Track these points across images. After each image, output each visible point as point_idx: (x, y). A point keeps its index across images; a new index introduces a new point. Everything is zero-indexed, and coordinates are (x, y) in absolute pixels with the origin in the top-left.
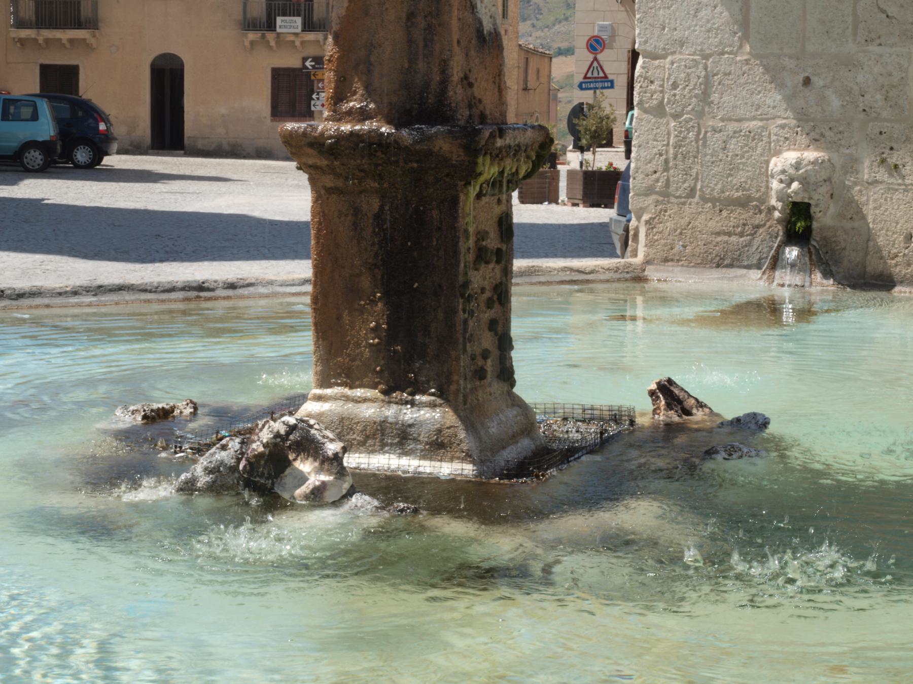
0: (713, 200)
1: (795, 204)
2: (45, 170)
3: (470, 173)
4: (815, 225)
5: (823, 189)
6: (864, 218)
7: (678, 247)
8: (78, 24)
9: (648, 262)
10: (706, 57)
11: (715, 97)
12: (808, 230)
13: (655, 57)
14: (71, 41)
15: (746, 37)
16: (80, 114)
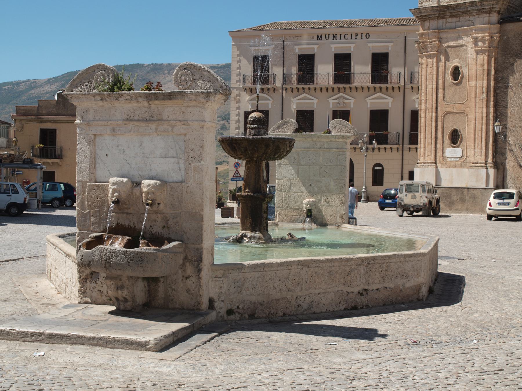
0: (292, 209)
1: (308, 209)
2: (59, 208)
3: (265, 200)
4: (312, 214)
5: (314, 206)
6: (322, 212)
7: (285, 218)
8: (55, 157)
9: (279, 222)
10: (290, 180)
11: (292, 188)
12: (311, 215)
13: (280, 180)
14: (52, 163)
15: (298, 176)
16: (68, 189)
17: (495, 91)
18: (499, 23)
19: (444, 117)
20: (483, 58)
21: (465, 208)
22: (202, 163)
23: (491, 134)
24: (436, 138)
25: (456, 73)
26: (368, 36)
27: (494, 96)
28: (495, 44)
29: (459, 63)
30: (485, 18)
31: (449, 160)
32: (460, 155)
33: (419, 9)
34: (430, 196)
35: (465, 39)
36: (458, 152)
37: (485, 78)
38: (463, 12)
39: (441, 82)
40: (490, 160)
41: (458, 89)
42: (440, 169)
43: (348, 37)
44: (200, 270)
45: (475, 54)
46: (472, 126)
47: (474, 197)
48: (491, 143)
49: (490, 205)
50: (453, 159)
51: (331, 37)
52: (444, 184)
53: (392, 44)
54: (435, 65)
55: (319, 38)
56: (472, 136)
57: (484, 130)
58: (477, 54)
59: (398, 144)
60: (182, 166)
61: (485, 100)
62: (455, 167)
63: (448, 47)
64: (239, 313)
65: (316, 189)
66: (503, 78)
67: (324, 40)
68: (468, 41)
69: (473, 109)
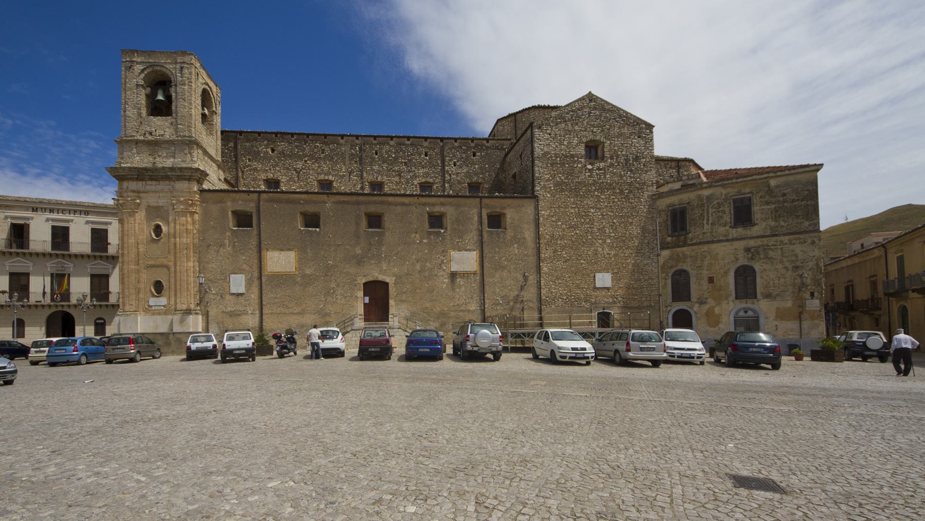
36: (163, 301)
62: (160, 314)
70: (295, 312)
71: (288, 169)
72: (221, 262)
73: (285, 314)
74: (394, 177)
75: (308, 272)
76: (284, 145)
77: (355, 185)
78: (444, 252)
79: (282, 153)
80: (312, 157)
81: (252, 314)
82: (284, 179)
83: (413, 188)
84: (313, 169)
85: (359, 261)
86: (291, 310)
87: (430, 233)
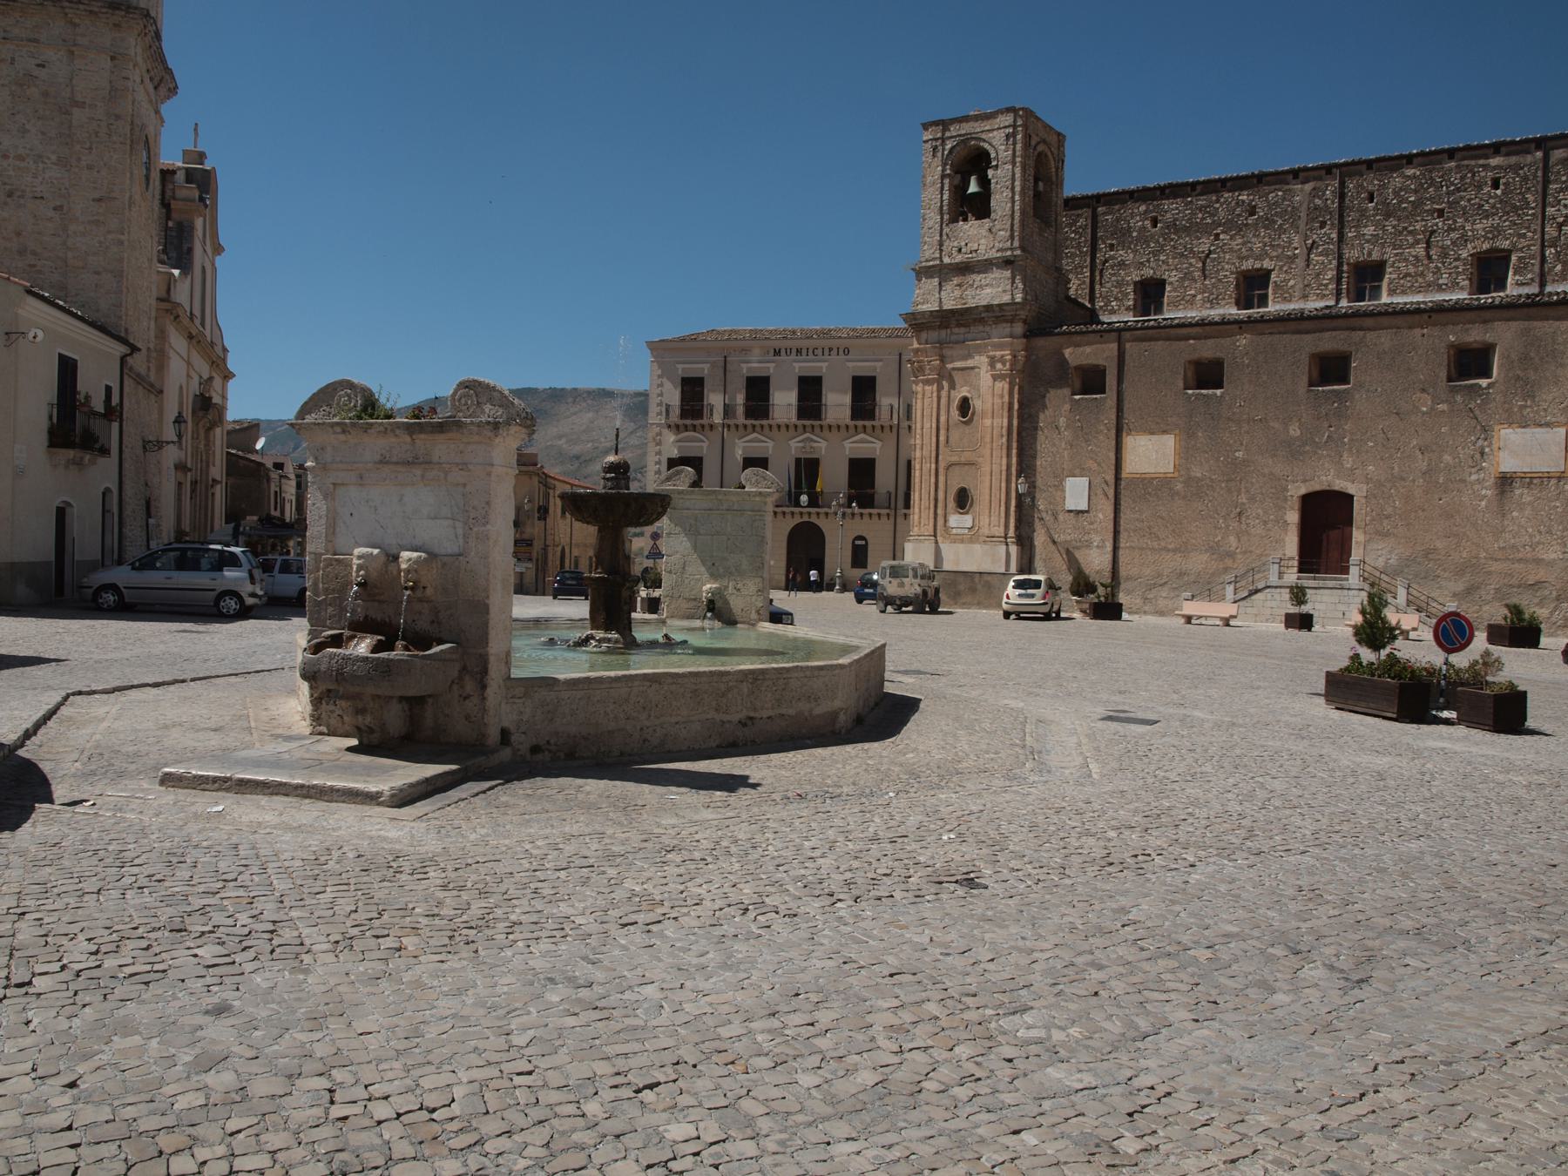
12: (714, 608)
17: (1019, 434)
18: (1025, 336)
19: (947, 469)
20: (1003, 386)
21: (976, 602)
22: (489, 527)
23: (1013, 495)
24: (936, 500)
25: (965, 405)
26: (847, 351)
27: (1018, 441)
28: (1019, 366)
29: (969, 392)
30: (1005, 328)
31: (954, 531)
32: (969, 524)
33: (913, 314)
34: (924, 583)
35: (977, 358)
36: (967, 520)
37: (1006, 414)
38: (975, 320)
39: (943, 419)
40: (1011, 533)
41: (967, 429)
42: (941, 546)
43: (819, 352)
44: (484, 687)
45: (991, 380)
46: (988, 484)
47: (988, 585)
48: (1013, 508)
49: (1008, 597)
50: (959, 531)
51: (794, 351)
52: (947, 566)
53: (881, 363)
54: (935, 394)
55: (777, 353)
56: (987, 497)
57: (1004, 490)
58: (995, 380)
59: (889, 507)
60: (460, 531)
61: (1005, 447)
62: (962, 541)
63: (954, 369)
64: (550, 751)
65: (721, 570)
66: (1030, 416)
67: (783, 357)
68: (981, 361)
69: (988, 459)
70: (1170, 547)
71: (1182, 255)
72: (1054, 455)
73: (1153, 549)
74: (1412, 246)
75: (1197, 472)
76: (1177, 208)
77: (1318, 274)
78: (1486, 431)
79: (1173, 227)
80: (1229, 226)
81: (1098, 547)
82: (1172, 277)
83: (1457, 267)
84: (1231, 250)
85: (1295, 451)
86: (1163, 544)
87: (1453, 390)
